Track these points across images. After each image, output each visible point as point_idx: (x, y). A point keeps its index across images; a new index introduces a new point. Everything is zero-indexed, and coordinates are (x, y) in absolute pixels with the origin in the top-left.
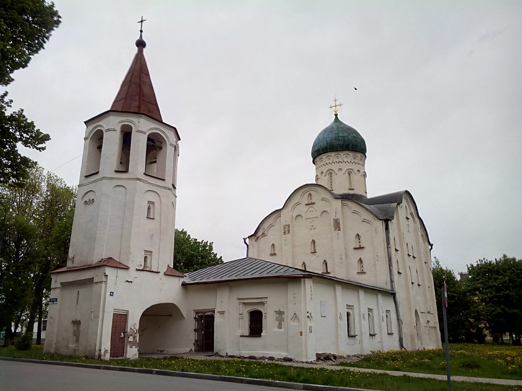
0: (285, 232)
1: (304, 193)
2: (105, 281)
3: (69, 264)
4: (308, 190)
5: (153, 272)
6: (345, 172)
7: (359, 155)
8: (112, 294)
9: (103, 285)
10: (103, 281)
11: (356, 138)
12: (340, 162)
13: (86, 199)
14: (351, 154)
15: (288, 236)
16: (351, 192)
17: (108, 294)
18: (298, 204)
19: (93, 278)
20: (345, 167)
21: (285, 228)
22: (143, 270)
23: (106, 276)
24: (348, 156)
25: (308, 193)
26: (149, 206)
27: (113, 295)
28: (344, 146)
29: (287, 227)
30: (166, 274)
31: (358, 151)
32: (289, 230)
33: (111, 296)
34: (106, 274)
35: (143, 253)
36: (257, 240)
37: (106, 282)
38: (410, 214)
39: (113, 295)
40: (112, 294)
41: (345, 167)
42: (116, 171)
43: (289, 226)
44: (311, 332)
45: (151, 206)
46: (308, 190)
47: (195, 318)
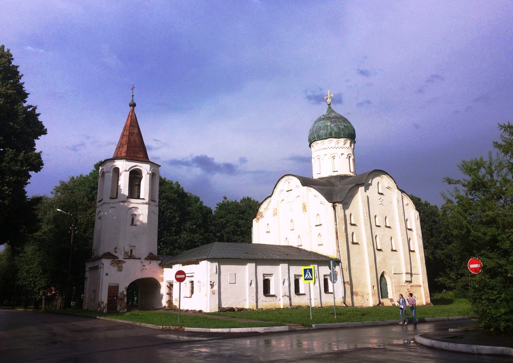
0: (274, 215)
1: (286, 181)
2: (102, 267)
3: (92, 257)
4: (288, 179)
5: (136, 259)
6: (330, 158)
7: (342, 140)
8: (107, 274)
9: (102, 270)
10: (101, 267)
11: (339, 125)
12: (325, 148)
13: (99, 216)
14: (335, 140)
15: (276, 217)
16: (335, 174)
17: (104, 274)
18: (282, 191)
19: (99, 265)
20: (330, 152)
21: (274, 211)
22: (129, 258)
23: (103, 264)
24: (332, 142)
25: (288, 182)
26: (133, 218)
27: (107, 275)
28: (328, 134)
29: (275, 210)
30: (146, 259)
31: (342, 136)
32: (276, 213)
33: (107, 276)
34: (103, 263)
35: (129, 248)
36: (258, 221)
37: (103, 268)
38: (387, 188)
39: (107, 275)
40: (107, 274)
41: (330, 152)
42: (111, 198)
43: (276, 209)
44: (214, 294)
45: (134, 217)
46: (288, 179)
47: (167, 286)
